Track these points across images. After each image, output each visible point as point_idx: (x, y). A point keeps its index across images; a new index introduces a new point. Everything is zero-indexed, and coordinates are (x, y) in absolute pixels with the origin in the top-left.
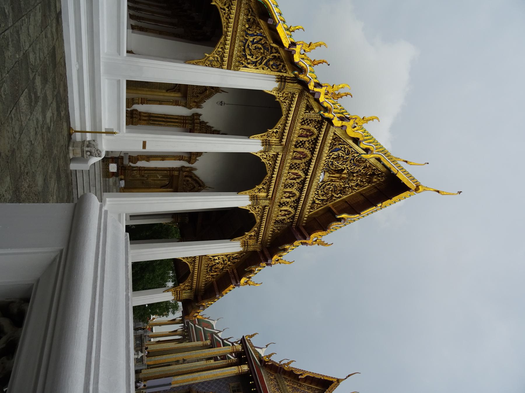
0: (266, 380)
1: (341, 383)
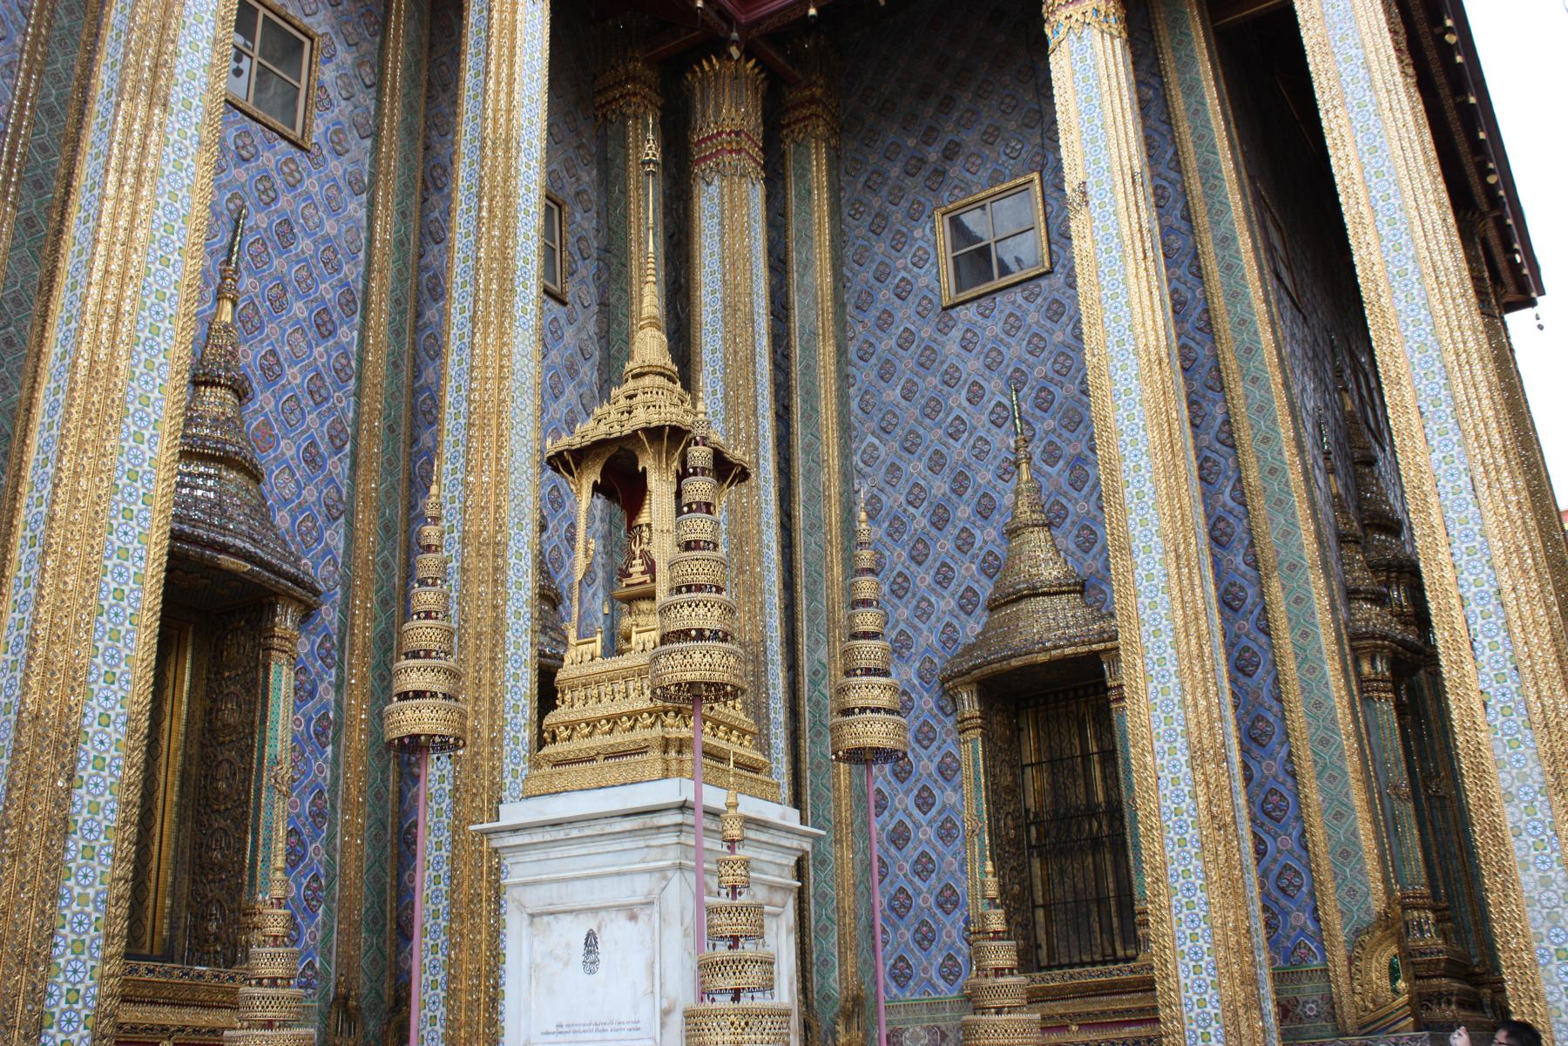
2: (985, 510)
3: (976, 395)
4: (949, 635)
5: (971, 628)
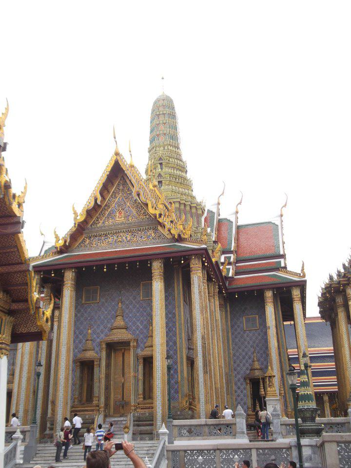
0: (89, 250)
1: (121, 152)
2: (250, 358)
3: (249, 343)
4: (245, 373)
5: (248, 372)
